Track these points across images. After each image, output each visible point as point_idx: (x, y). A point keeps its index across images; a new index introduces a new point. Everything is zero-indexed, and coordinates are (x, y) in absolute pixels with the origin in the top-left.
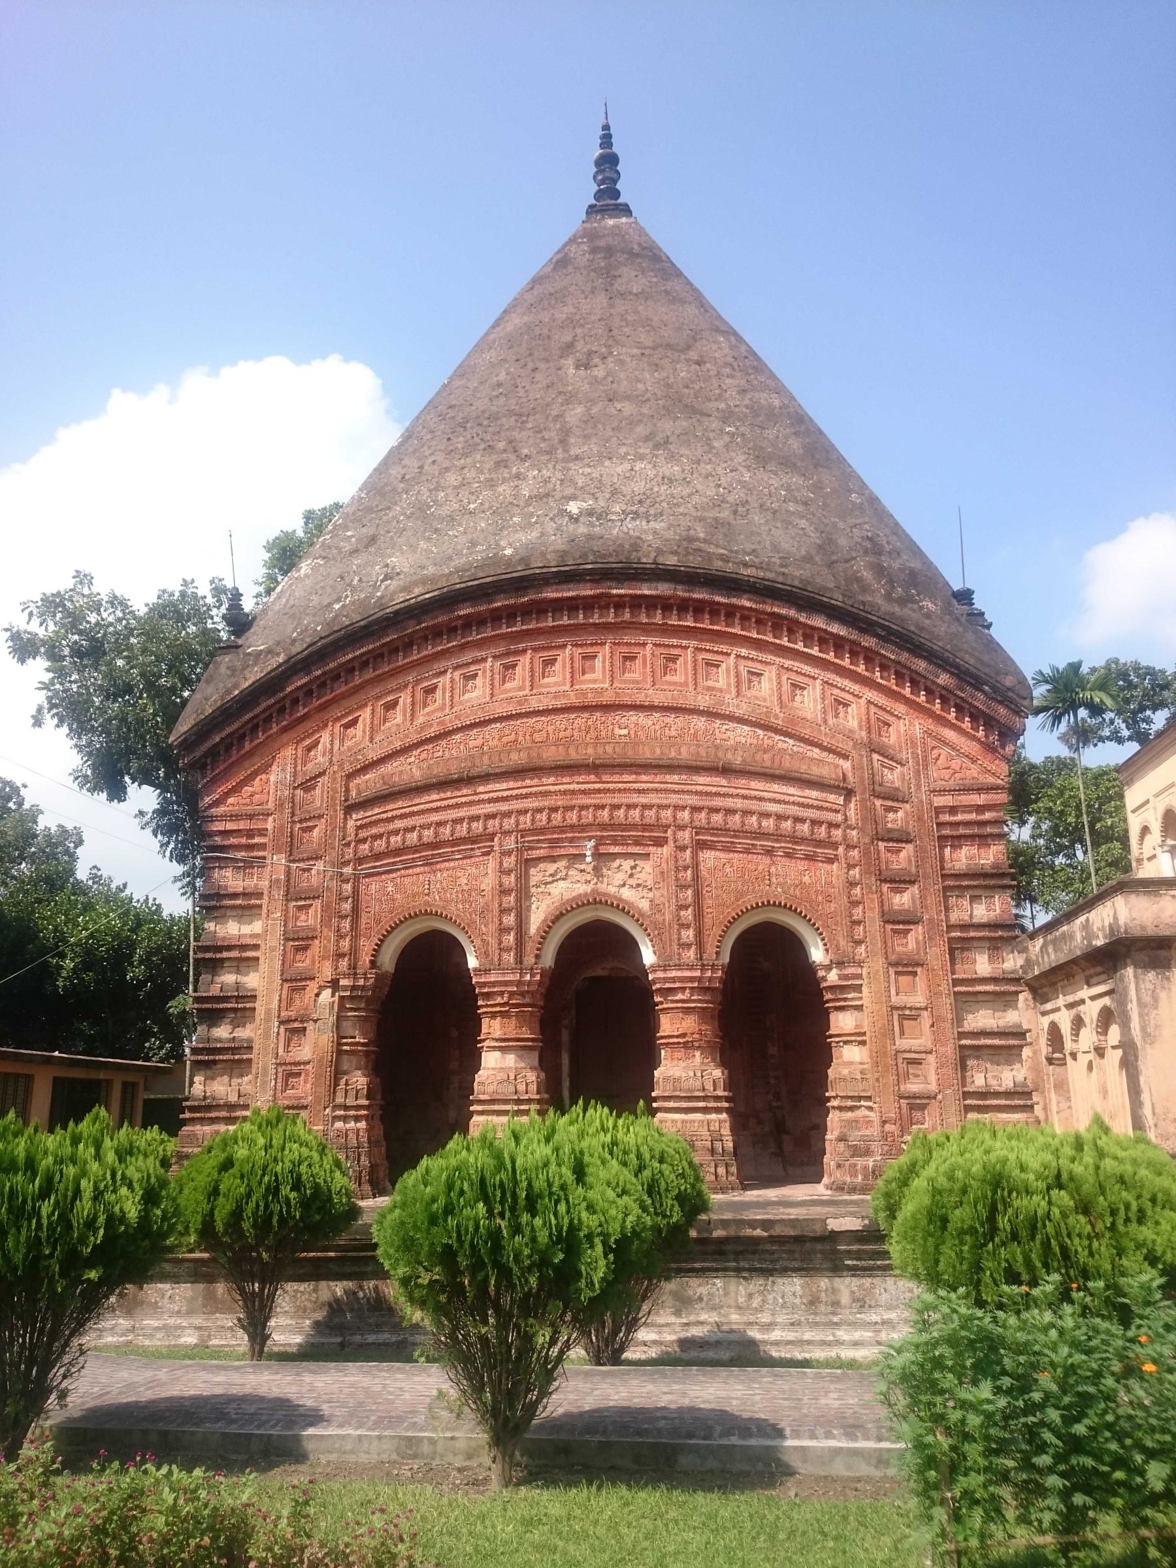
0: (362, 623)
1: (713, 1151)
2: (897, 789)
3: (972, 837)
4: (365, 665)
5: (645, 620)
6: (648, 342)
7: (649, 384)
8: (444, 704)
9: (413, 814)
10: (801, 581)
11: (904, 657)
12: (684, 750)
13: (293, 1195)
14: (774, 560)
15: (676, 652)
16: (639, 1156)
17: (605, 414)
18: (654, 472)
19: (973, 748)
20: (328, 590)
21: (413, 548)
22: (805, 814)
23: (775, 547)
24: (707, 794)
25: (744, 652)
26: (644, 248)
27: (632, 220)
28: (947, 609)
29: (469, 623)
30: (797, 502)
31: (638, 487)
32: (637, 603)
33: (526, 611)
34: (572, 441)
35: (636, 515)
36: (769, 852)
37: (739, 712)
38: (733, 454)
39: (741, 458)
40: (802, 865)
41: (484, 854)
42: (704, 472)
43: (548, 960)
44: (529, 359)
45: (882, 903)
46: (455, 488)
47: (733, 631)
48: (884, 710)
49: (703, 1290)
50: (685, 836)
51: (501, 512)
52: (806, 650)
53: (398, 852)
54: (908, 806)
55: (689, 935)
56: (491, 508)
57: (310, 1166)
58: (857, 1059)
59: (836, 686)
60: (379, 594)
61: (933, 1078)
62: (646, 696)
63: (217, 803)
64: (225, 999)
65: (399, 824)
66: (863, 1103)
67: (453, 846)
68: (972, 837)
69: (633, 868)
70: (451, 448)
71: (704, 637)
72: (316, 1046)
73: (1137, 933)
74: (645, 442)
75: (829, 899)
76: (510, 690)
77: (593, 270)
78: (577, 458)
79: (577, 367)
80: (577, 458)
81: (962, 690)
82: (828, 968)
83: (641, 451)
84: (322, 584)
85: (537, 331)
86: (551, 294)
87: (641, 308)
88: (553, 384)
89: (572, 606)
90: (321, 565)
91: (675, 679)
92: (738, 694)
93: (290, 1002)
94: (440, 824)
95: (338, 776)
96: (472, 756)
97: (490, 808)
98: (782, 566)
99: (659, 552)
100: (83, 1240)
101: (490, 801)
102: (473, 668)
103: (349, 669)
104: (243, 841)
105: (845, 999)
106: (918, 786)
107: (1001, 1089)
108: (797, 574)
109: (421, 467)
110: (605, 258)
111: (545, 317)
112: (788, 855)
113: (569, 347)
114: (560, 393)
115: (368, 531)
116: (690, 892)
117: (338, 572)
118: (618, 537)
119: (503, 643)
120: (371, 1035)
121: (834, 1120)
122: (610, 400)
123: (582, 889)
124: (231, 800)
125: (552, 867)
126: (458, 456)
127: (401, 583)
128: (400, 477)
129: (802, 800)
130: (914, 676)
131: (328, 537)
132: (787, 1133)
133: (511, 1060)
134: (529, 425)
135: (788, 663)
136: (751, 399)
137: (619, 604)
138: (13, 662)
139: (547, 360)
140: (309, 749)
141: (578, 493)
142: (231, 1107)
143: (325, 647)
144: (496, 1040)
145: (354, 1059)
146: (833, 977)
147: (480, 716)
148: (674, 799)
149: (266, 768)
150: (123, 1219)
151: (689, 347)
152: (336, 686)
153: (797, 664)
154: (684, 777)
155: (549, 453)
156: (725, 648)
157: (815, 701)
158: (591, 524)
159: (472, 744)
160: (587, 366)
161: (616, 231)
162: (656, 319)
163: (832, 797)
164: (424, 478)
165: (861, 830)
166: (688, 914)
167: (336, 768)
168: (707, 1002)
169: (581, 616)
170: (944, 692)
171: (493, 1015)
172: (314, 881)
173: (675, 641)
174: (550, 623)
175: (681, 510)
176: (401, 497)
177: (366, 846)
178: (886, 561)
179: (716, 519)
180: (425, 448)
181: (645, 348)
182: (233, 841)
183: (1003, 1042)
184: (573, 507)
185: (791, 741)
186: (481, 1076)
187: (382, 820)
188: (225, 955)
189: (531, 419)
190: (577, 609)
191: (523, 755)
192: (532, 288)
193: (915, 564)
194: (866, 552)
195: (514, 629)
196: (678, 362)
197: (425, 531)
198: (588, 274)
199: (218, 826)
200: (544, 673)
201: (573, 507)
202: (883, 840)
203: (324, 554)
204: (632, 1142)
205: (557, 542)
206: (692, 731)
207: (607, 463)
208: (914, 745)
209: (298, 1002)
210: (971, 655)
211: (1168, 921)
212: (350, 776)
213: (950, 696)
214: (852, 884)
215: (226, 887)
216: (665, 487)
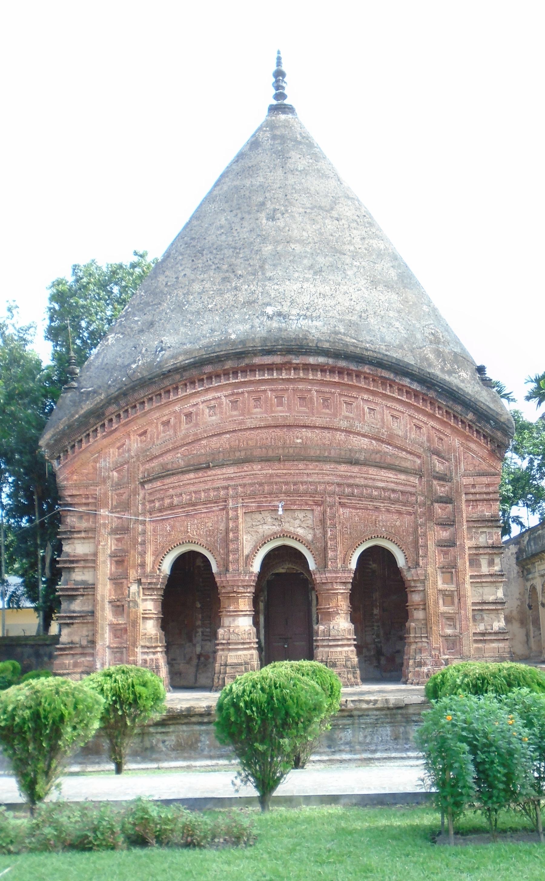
6: (308, 205)
7: (309, 232)
9: (179, 486)
10: (397, 359)
11: (450, 403)
12: (333, 452)
14: (382, 347)
18: (315, 290)
19: (484, 453)
21: (177, 332)
22: (398, 488)
23: (383, 340)
24: (346, 477)
25: (366, 397)
26: (303, 138)
31: (306, 299)
32: (307, 367)
34: (267, 267)
36: (377, 508)
38: (359, 280)
40: (395, 517)
42: (342, 290)
44: (238, 211)
46: (199, 293)
47: (360, 385)
48: (440, 431)
52: (399, 397)
56: (221, 308)
59: (415, 418)
62: (312, 421)
70: (194, 267)
71: (344, 388)
76: (235, 416)
78: (270, 279)
79: (268, 219)
81: (480, 423)
83: (307, 276)
86: (250, 167)
87: (303, 181)
88: (254, 229)
89: (270, 368)
90: (121, 338)
98: (386, 350)
99: (319, 340)
101: (224, 479)
105: (416, 587)
106: (456, 473)
108: (396, 354)
110: (280, 144)
111: (247, 183)
112: (388, 511)
113: (263, 204)
118: (295, 330)
119: (230, 388)
122: (288, 242)
123: (276, 528)
125: (259, 517)
126: (199, 273)
128: (164, 283)
129: (396, 480)
130: (456, 414)
131: (123, 319)
132: (383, 655)
134: (241, 256)
135: (389, 404)
137: (296, 368)
139: (249, 213)
141: (272, 301)
147: (218, 431)
148: (327, 478)
151: (332, 209)
154: (332, 466)
156: (354, 394)
159: (213, 446)
160: (273, 219)
162: (312, 188)
163: (412, 479)
164: (180, 285)
168: (343, 589)
170: (470, 423)
173: (327, 390)
174: (258, 378)
175: (330, 314)
176: (166, 297)
178: (441, 347)
179: (350, 320)
180: (179, 265)
183: (494, 608)
184: (270, 310)
185: (391, 448)
187: (161, 490)
190: (272, 370)
192: (237, 161)
193: (457, 350)
194: (431, 342)
195: (237, 381)
196: (326, 218)
197: (183, 321)
201: (270, 310)
202: (437, 502)
205: (261, 332)
207: (288, 283)
208: (455, 451)
210: (484, 404)
213: (473, 425)
216: (321, 300)
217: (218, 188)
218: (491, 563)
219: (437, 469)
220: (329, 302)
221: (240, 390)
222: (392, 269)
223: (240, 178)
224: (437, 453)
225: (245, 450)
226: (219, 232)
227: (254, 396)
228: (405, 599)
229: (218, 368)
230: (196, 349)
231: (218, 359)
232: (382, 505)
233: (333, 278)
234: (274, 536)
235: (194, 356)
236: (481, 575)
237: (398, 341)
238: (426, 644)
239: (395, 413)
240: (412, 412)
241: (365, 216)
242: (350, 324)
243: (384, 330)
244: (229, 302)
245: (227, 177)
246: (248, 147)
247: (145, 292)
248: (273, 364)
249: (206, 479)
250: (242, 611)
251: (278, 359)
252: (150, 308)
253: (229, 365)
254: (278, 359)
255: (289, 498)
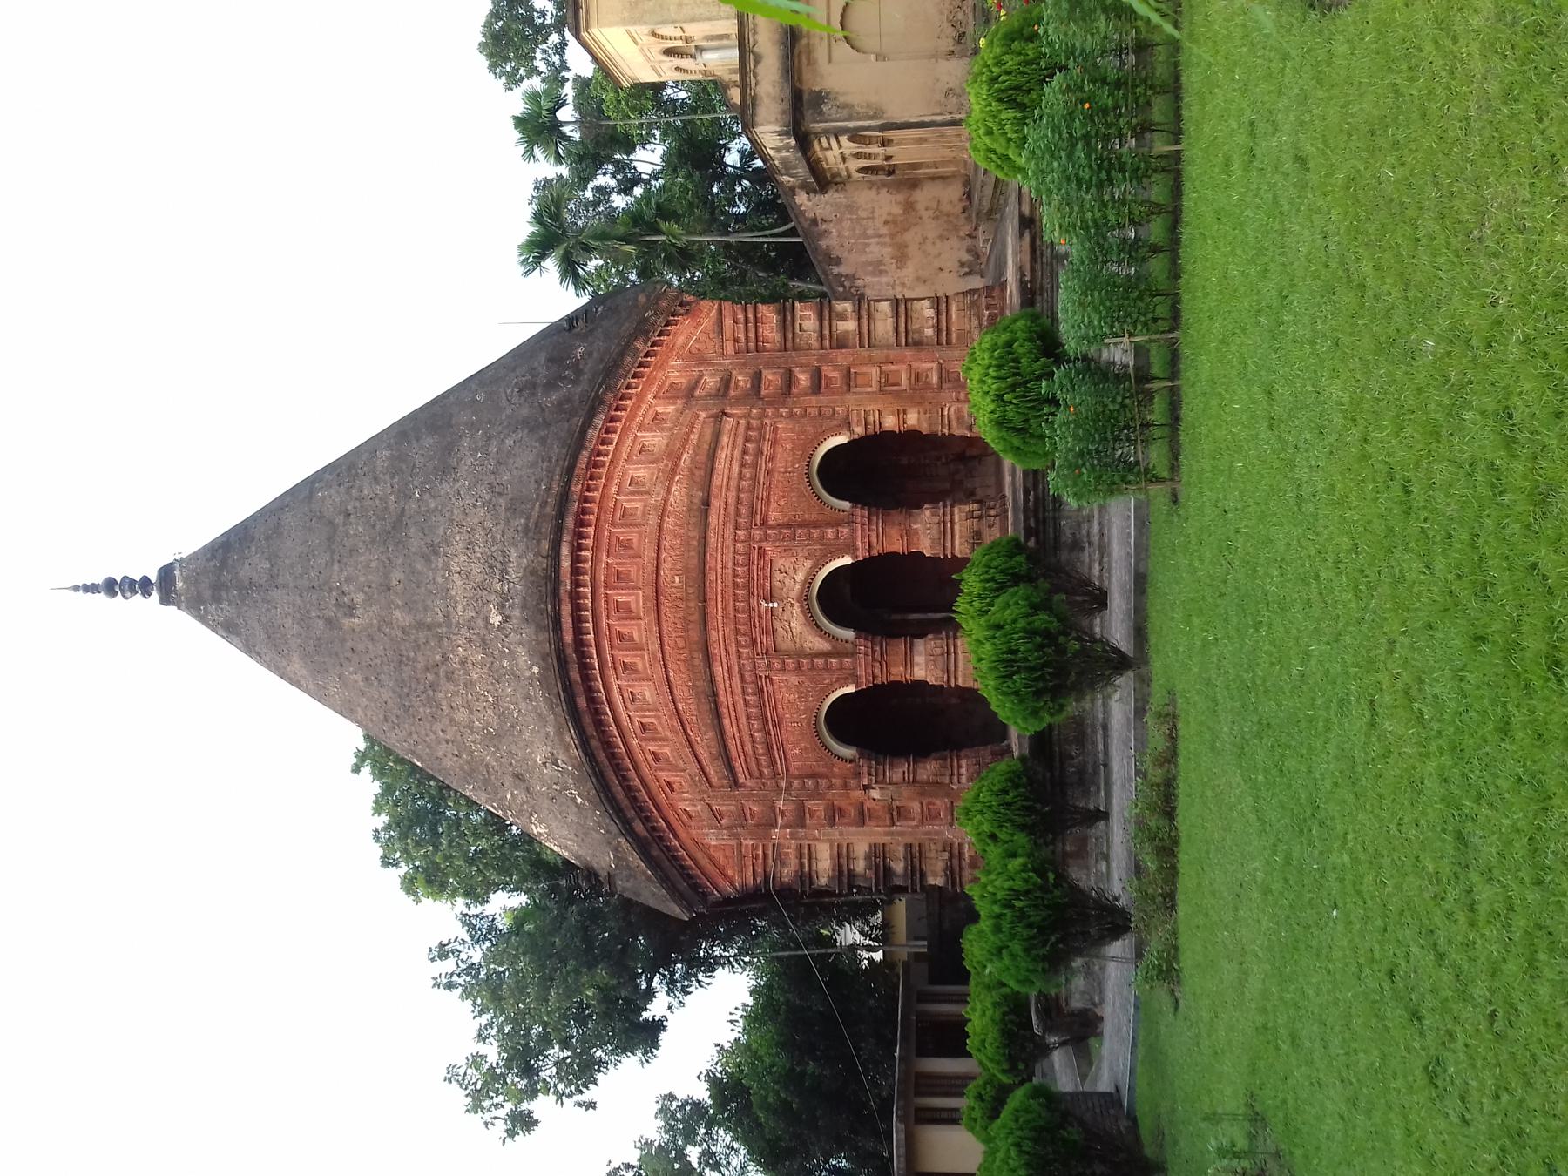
0: (594, 780)
1: (980, 518)
2: (722, 379)
3: (756, 327)
4: (625, 778)
5: (590, 564)
6: (327, 557)
8: (655, 716)
10: (563, 447)
12: (691, 534)
13: (1011, 794)
14: (544, 467)
15: (614, 541)
16: (987, 581)
17: (403, 593)
20: (564, 808)
22: (741, 446)
23: (533, 465)
24: (726, 516)
26: (213, 557)
27: (177, 565)
28: (583, 337)
29: (592, 700)
30: (489, 445)
31: (477, 568)
32: (576, 571)
33: (582, 655)
35: (504, 571)
37: (663, 493)
38: (442, 492)
39: (445, 485)
40: (779, 449)
41: (772, 683)
42: (461, 517)
43: (849, 634)
44: (342, 656)
45: (806, 394)
46: (471, 713)
49: (1068, 532)
50: (757, 533)
51: (497, 676)
53: (769, 748)
54: (734, 373)
55: (830, 532)
57: (994, 785)
58: (916, 415)
60: (570, 768)
61: (928, 365)
62: (649, 562)
63: (732, 884)
64: (877, 866)
65: (748, 748)
66: (946, 413)
67: (765, 706)
68: (756, 327)
69: (781, 572)
72: (910, 798)
73: (788, 118)
74: (430, 561)
75: (803, 432)
76: (644, 664)
77: (243, 601)
78: (447, 616)
79: (353, 616)
80: (447, 616)
82: (852, 432)
83: (440, 565)
84: (558, 814)
85: (311, 649)
86: (269, 637)
87: (287, 561)
89: (577, 620)
91: (635, 541)
92: (647, 493)
93: (878, 818)
94: (749, 717)
95: (711, 794)
96: (697, 693)
97: (736, 679)
98: (550, 460)
99: (538, 554)
100: (1035, 884)
101: (730, 679)
102: (625, 695)
103: (628, 789)
104: (761, 861)
106: (720, 364)
107: (935, 319)
108: (556, 450)
109: (447, 742)
111: (294, 643)
112: (772, 459)
113: (329, 622)
114: (379, 630)
115: (508, 780)
116: (799, 531)
117: (547, 801)
119: (606, 672)
120: (902, 760)
121: (957, 432)
122: (389, 589)
123: (796, 609)
124: (730, 873)
126: (440, 712)
127: (561, 752)
128: (455, 758)
129: (730, 448)
133: (920, 659)
136: (384, 474)
137: (577, 584)
138: (537, 1131)
139: (343, 641)
140: (690, 817)
141: (482, 616)
142: (951, 859)
143: (613, 808)
144: (906, 669)
145: (919, 771)
146: (859, 431)
147: (665, 689)
148: (728, 542)
149: (705, 849)
150: (1025, 865)
151: (331, 523)
152: (641, 799)
153: (624, 449)
155: (441, 639)
156: (611, 504)
157: (653, 436)
158: (512, 606)
159: (687, 694)
161: (193, 579)
163: (728, 426)
165: (752, 407)
166: (815, 532)
167: (705, 796)
168: (878, 519)
169: (586, 613)
170: (649, 344)
171: (888, 672)
172: (791, 807)
173: (605, 542)
177: (765, 771)
179: (507, 509)
181: (333, 561)
182: (760, 870)
184: (496, 619)
185: (685, 455)
186: (931, 681)
187: (745, 760)
188: (845, 868)
189: (405, 653)
191: (695, 655)
192: (259, 654)
193: (542, 357)
194: (533, 394)
195: (596, 664)
196: (347, 533)
197: (514, 735)
198: (247, 605)
199: (750, 881)
200: (629, 640)
201: (496, 619)
202: (759, 391)
203: (528, 815)
204: (978, 585)
205: (528, 632)
206: (677, 528)
209: (880, 813)
211: (777, 89)
212: (711, 786)
214: (791, 415)
215: (796, 872)
216: (476, 547)
217: (303, 682)
218: (842, 317)
219: (713, 392)
220: (479, 535)
221: (609, 658)
222: (421, 441)
223: (286, 652)
224: (692, 388)
225: (690, 651)
226: (376, 683)
227: (616, 641)
228: (891, 434)
229: (579, 689)
230: (555, 719)
231: (568, 689)
232: (763, 468)
233: (441, 529)
234: (807, 611)
235: (564, 722)
236: (860, 332)
237: (534, 444)
238: (952, 409)
239: (637, 448)
240: (634, 426)
241: (338, 475)
242: (512, 509)
243: (519, 463)
244: (484, 673)
245: (285, 668)
246: (233, 637)
247: (469, 784)
248: (572, 616)
249: (730, 703)
250: (906, 653)
251: (566, 610)
252: (493, 777)
253: (575, 675)
254: (566, 610)
255: (756, 594)
